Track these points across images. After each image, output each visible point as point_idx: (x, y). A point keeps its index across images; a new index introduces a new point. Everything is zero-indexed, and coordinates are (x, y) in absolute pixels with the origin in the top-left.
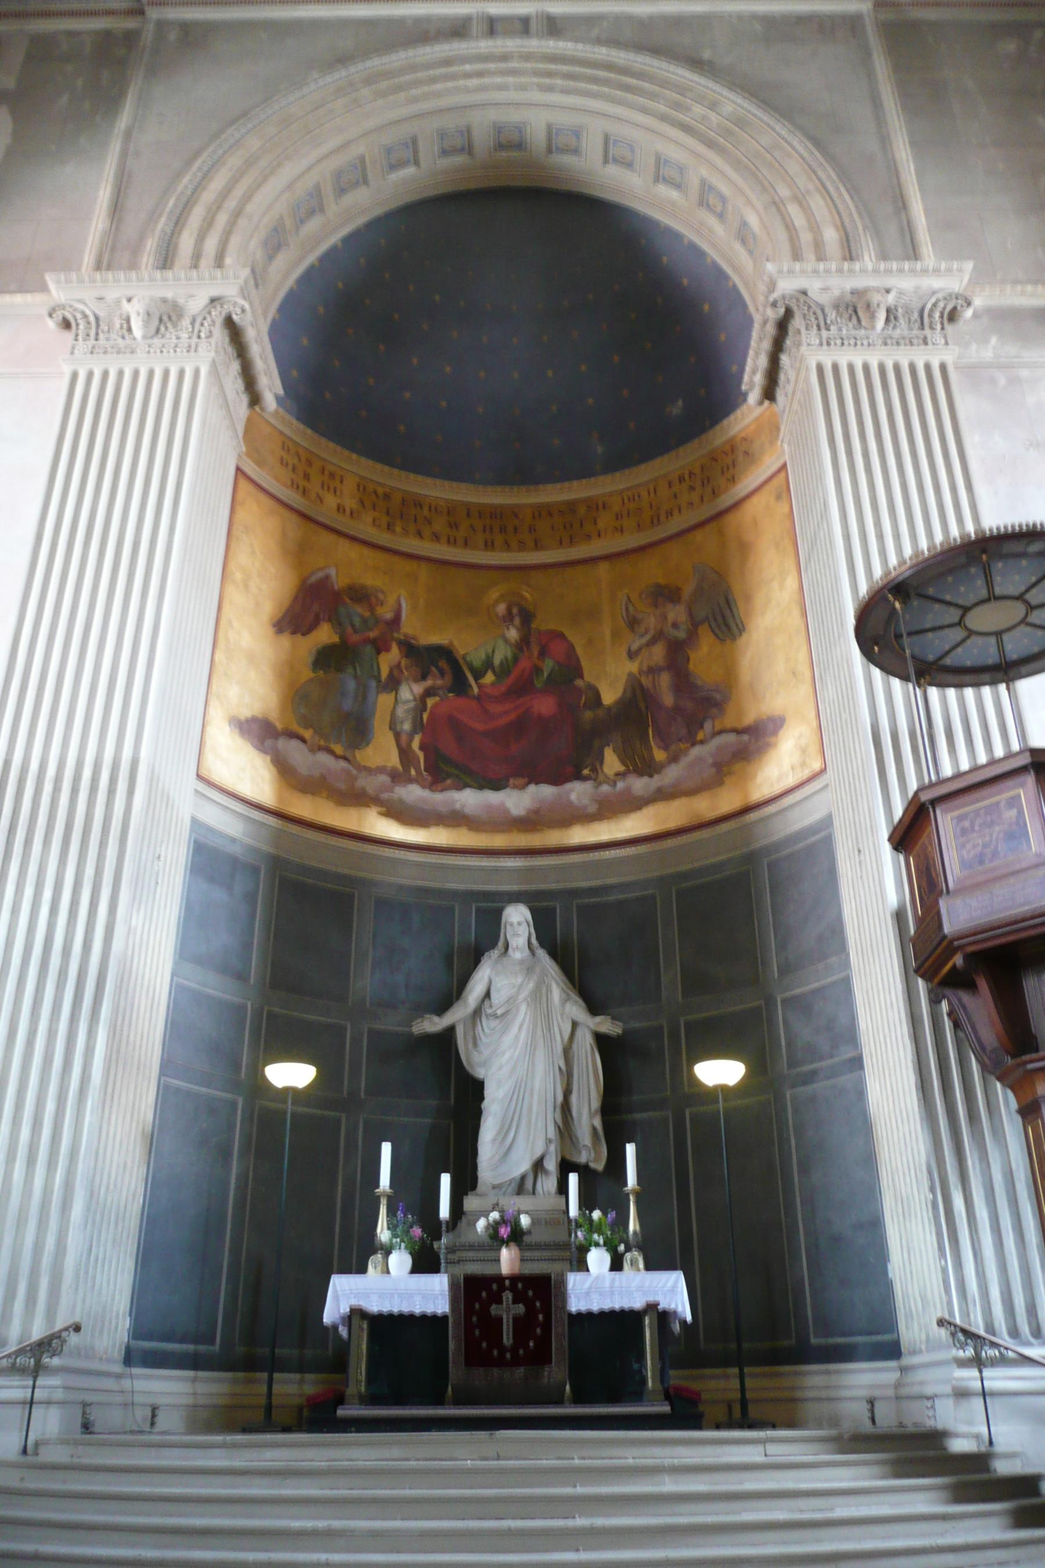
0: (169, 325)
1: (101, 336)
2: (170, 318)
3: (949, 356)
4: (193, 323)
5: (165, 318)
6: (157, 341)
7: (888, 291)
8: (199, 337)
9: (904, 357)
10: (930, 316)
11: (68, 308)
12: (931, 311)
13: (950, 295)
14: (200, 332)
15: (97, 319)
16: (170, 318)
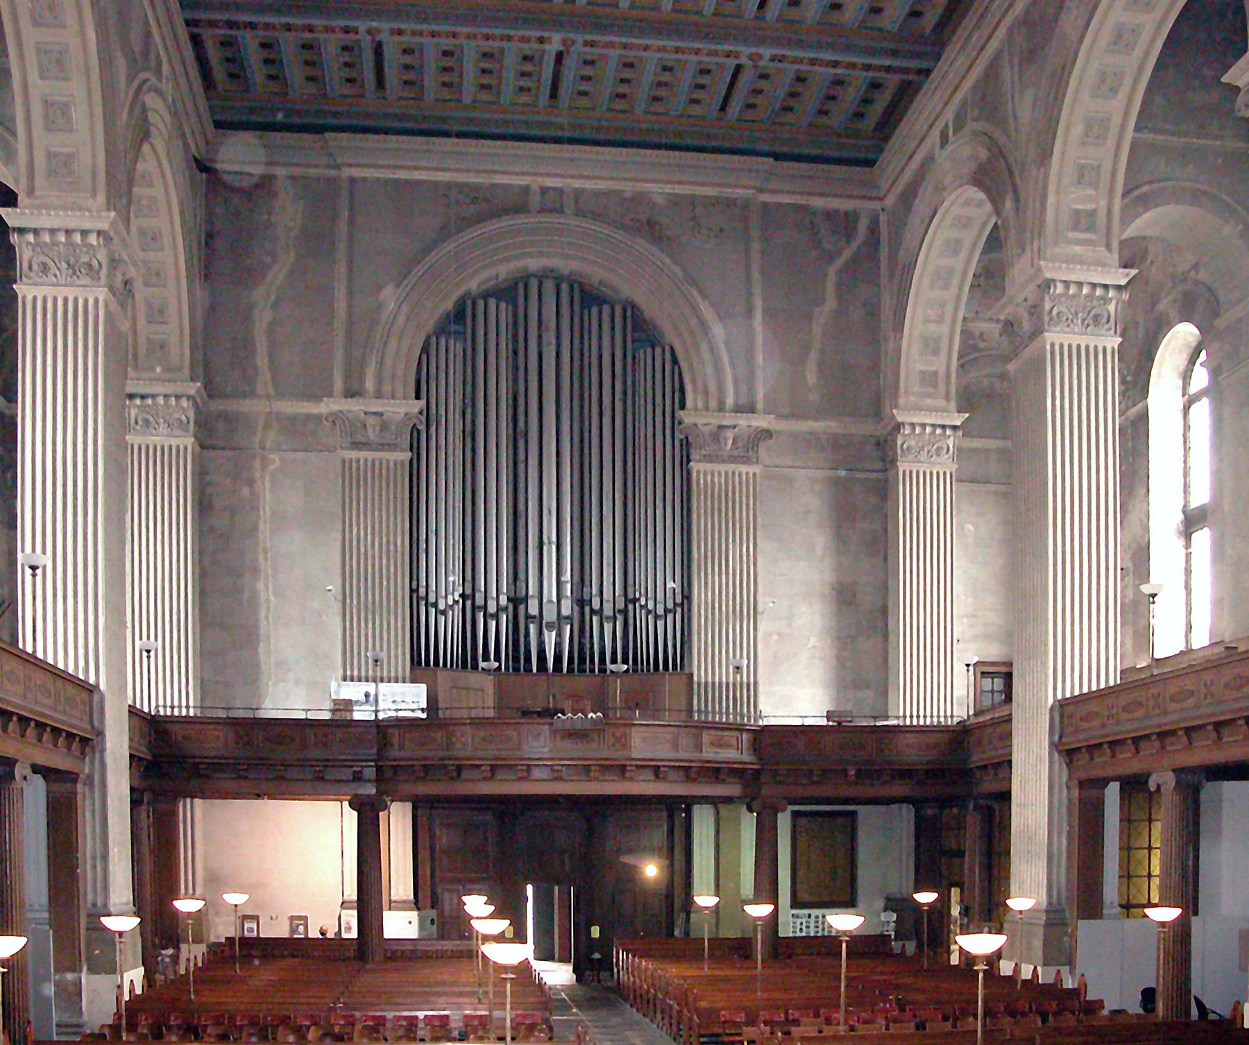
3: (757, 469)
7: (734, 427)
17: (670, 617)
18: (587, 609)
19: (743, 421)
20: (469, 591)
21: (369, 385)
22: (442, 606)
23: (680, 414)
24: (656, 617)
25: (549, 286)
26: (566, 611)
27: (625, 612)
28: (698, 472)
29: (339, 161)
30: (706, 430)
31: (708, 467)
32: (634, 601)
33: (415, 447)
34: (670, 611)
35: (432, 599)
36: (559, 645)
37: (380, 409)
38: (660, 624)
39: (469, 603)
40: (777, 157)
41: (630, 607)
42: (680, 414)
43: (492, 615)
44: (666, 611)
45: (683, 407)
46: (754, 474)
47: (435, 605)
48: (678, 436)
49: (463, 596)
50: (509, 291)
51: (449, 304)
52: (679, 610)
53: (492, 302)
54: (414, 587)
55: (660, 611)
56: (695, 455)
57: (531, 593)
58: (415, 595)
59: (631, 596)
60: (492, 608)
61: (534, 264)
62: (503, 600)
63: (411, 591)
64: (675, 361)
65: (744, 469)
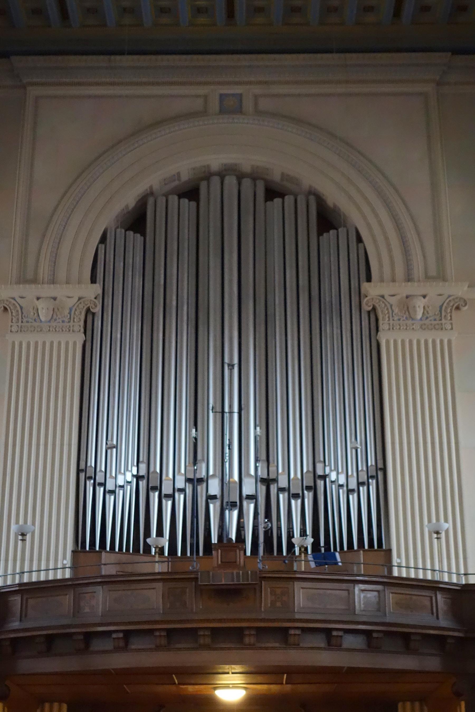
0: (58, 313)
1: (25, 320)
2: (58, 309)
4: (70, 313)
5: (56, 310)
6: (53, 324)
7: (424, 297)
8: (74, 321)
9: (430, 336)
10: (446, 311)
11: (5, 302)
12: (446, 308)
13: (457, 298)
14: (74, 318)
15: (21, 308)
16: (58, 309)
17: (363, 490)
18: (273, 489)
19: (434, 290)
20: (143, 472)
21: (44, 270)
22: (110, 486)
23: (365, 286)
24: (350, 491)
25: (231, 181)
26: (248, 489)
27: (313, 489)
28: (388, 342)
29: (25, 81)
30: (393, 300)
31: (400, 336)
32: (324, 477)
33: (88, 329)
34: (363, 484)
35: (100, 478)
36: (240, 528)
37: (53, 295)
38: (353, 498)
39: (143, 484)
40: (456, 52)
41: (320, 483)
42: (365, 286)
43: (167, 496)
44: (360, 484)
45: (369, 279)
46: (449, 342)
47: (103, 484)
48: (366, 308)
49: (138, 478)
50: (191, 193)
51: (129, 200)
52: (373, 482)
53: (174, 199)
54: (82, 466)
55: (353, 484)
56: (383, 325)
57: (211, 472)
58: (82, 476)
59: (320, 472)
60: (167, 489)
61: (216, 161)
62: (180, 483)
63: (79, 471)
64: (359, 239)
65: (438, 336)
